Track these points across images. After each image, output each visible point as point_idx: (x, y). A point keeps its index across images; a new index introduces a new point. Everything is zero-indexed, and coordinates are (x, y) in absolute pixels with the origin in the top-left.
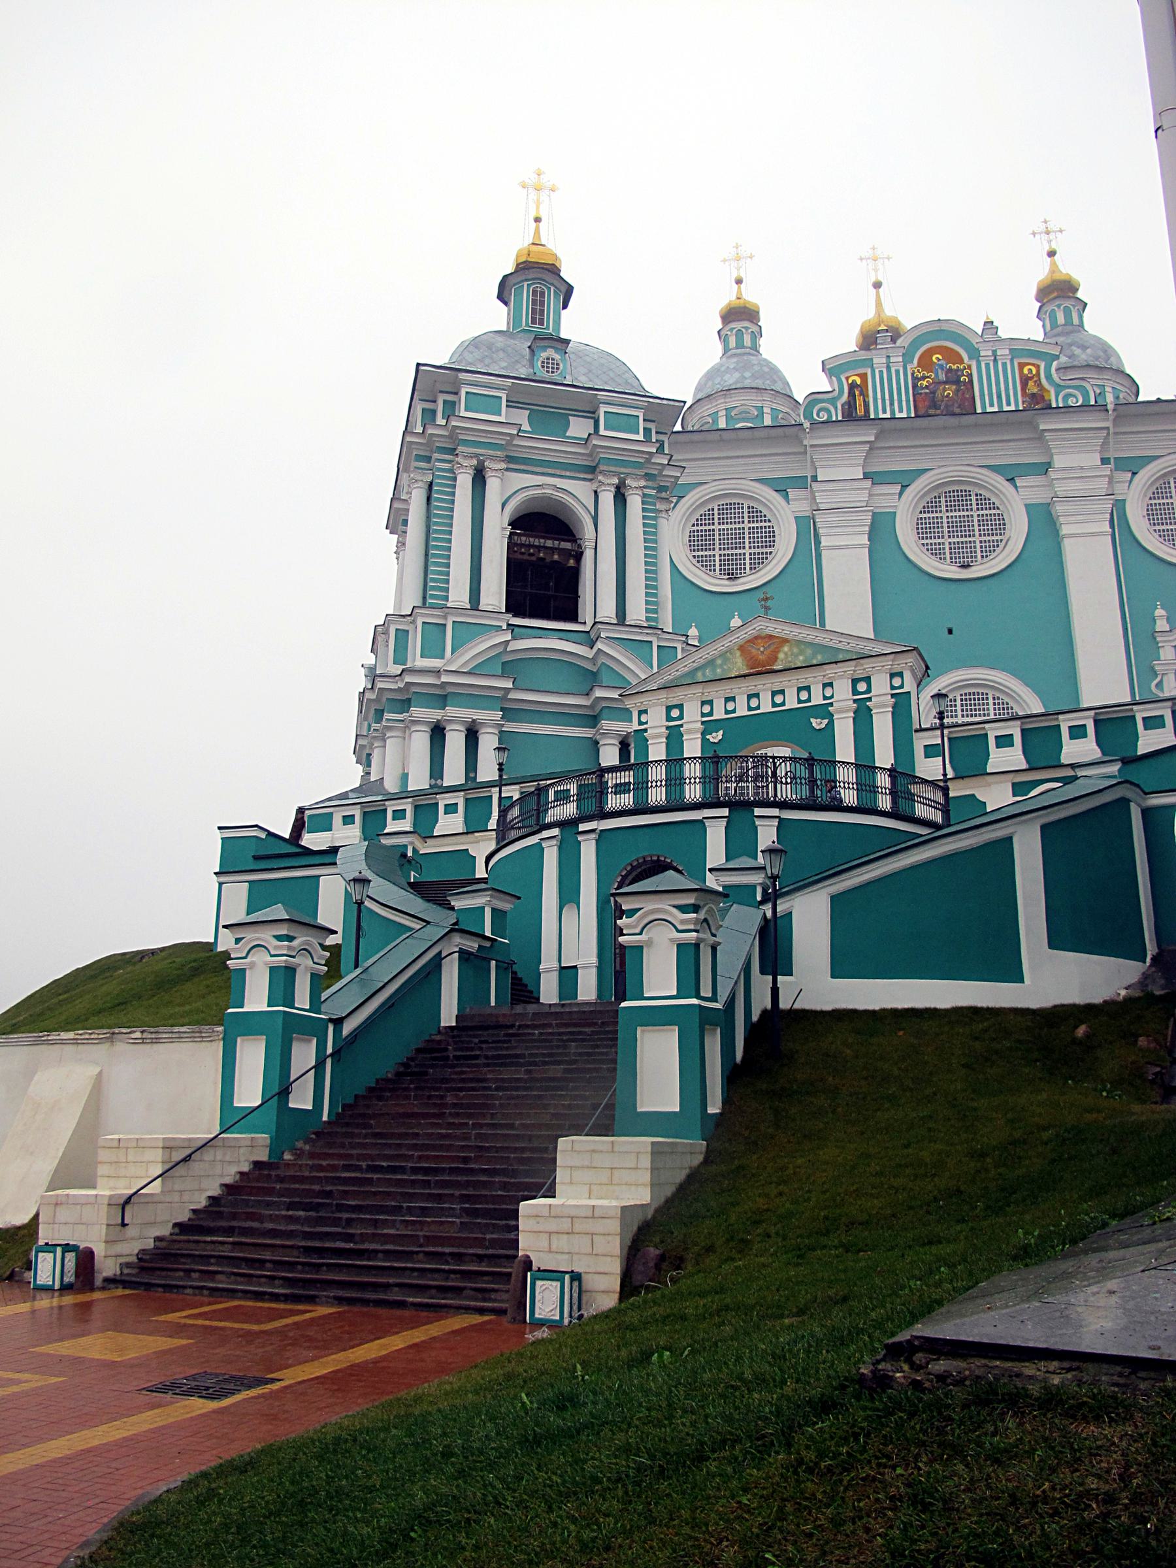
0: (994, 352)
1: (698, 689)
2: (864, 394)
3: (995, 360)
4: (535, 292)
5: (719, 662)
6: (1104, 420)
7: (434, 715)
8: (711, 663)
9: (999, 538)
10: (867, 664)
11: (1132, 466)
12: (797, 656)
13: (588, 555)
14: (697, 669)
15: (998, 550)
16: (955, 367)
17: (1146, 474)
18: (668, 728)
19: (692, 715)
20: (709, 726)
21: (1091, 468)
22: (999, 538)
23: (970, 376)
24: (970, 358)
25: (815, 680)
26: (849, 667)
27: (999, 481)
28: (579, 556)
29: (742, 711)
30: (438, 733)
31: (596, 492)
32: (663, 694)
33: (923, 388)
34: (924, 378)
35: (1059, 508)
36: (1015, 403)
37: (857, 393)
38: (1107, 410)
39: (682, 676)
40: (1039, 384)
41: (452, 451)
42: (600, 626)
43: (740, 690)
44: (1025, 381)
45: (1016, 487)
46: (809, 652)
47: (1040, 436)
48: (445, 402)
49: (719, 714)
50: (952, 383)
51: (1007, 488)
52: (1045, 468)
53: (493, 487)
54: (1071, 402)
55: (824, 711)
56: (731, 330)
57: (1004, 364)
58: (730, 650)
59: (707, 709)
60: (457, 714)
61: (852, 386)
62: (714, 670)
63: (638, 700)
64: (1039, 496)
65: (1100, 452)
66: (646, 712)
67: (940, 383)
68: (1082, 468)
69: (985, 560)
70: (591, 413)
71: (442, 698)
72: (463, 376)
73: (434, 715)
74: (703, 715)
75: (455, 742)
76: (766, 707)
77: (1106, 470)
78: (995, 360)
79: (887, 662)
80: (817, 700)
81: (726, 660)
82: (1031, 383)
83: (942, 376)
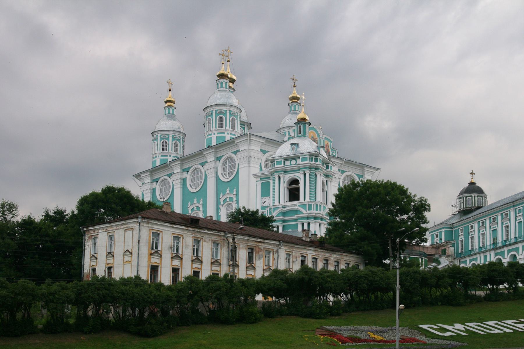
3: (322, 139)
11: (343, 172)
17: (345, 174)
21: (336, 171)
23: (317, 141)
24: (318, 137)
31: (327, 181)
40: (328, 146)
41: (316, 169)
56: (224, 81)
57: (323, 140)
65: (339, 167)
72: (320, 155)
78: (322, 139)
82: (327, 147)
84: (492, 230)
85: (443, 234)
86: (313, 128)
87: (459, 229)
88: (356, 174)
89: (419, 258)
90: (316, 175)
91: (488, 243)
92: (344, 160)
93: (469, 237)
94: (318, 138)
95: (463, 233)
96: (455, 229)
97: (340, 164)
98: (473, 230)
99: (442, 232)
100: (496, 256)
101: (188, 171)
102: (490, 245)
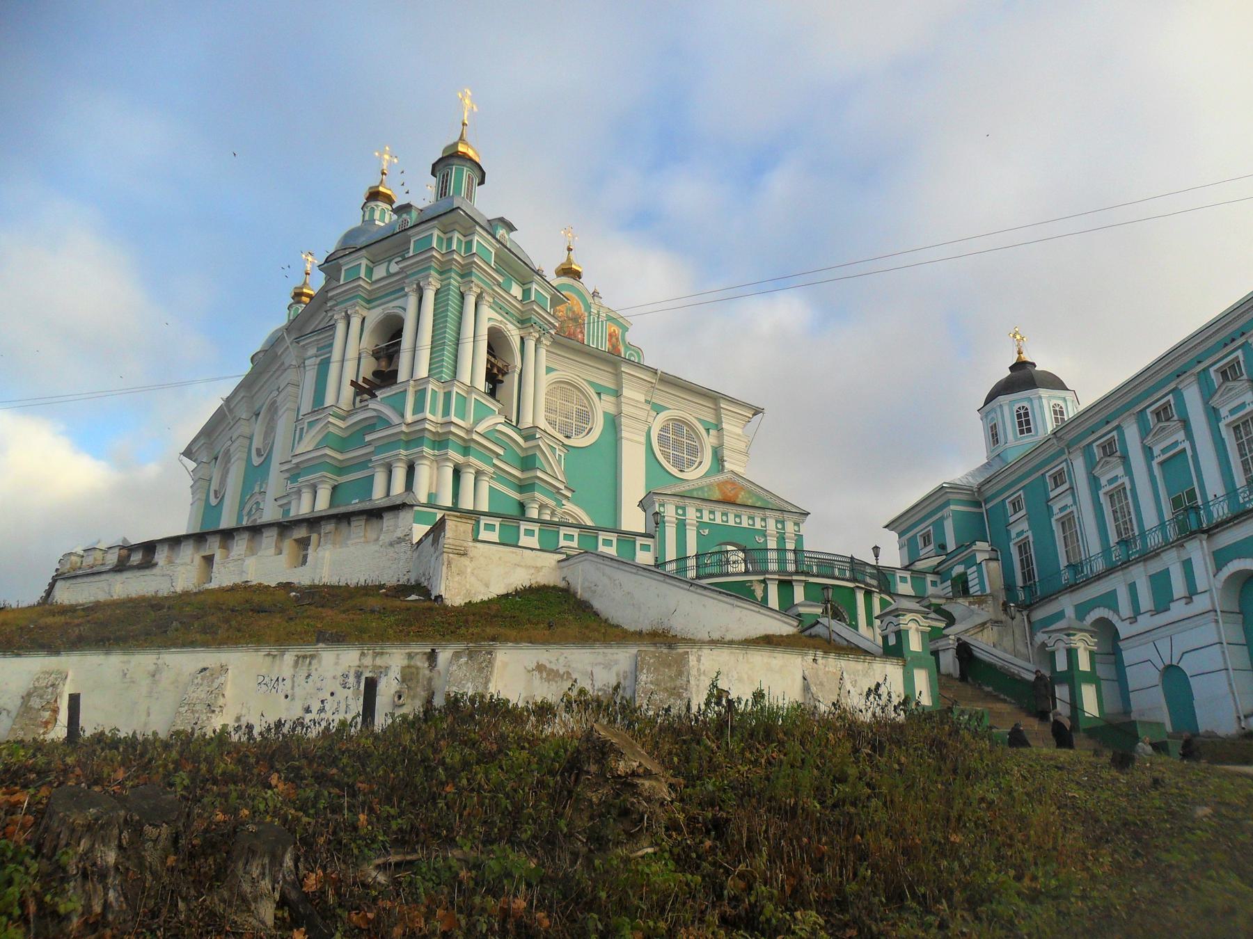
0: (598, 312)
1: (698, 502)
3: (598, 318)
4: (469, 177)
5: (706, 489)
6: (653, 378)
7: (459, 458)
8: (701, 488)
9: (585, 426)
10: (786, 515)
11: (658, 409)
12: (748, 499)
14: (696, 489)
15: (584, 433)
17: (664, 415)
18: (677, 518)
19: (691, 514)
20: (701, 525)
22: (585, 426)
24: (585, 310)
25: (758, 514)
26: (777, 514)
27: (592, 392)
29: (718, 521)
30: (457, 473)
31: (522, 338)
32: (677, 499)
35: (623, 420)
36: (606, 347)
38: (656, 373)
39: (685, 491)
40: (617, 339)
42: (538, 430)
43: (720, 509)
44: (610, 335)
45: (600, 399)
46: (754, 499)
47: (618, 375)
49: (706, 519)
51: (595, 397)
52: (617, 394)
53: (487, 312)
54: (632, 359)
55: (764, 533)
58: (711, 484)
59: (699, 515)
62: (700, 493)
63: (661, 498)
64: (611, 409)
66: (663, 505)
68: (637, 401)
69: (577, 437)
70: (524, 283)
72: (478, 228)
73: (459, 458)
74: (697, 517)
75: (468, 479)
76: (731, 522)
77: (648, 407)
78: (598, 318)
79: (795, 517)
80: (758, 526)
81: (710, 490)
82: (614, 339)
84: (1161, 464)
85: (949, 526)
86: (572, 286)
87: (1003, 501)
88: (699, 420)
89: (853, 590)
90: (462, 296)
91: (1150, 520)
92: (659, 372)
93: (1053, 520)
94: (586, 314)
95: (1023, 512)
96: (989, 506)
97: (650, 385)
98: (1066, 486)
99: (942, 519)
100: (1219, 569)
101: (259, 414)
102: (1162, 525)
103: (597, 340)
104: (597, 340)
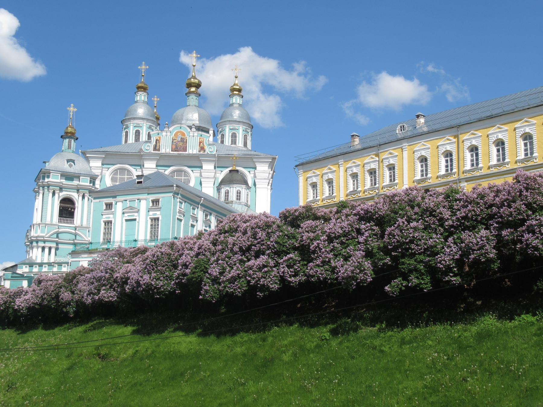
2: (159, 143)
13: (76, 209)
16: (183, 137)
23: (187, 140)
28: (74, 209)
33: (174, 142)
34: (175, 140)
37: (158, 142)
40: (203, 144)
44: (200, 143)
48: (47, 175)
50: (182, 142)
60: (48, 244)
61: (157, 140)
67: (179, 141)
71: (45, 241)
72: (51, 171)
73: (43, 245)
82: (201, 144)
83: (180, 139)
94: (188, 137)
103: (193, 147)
104: (193, 147)
